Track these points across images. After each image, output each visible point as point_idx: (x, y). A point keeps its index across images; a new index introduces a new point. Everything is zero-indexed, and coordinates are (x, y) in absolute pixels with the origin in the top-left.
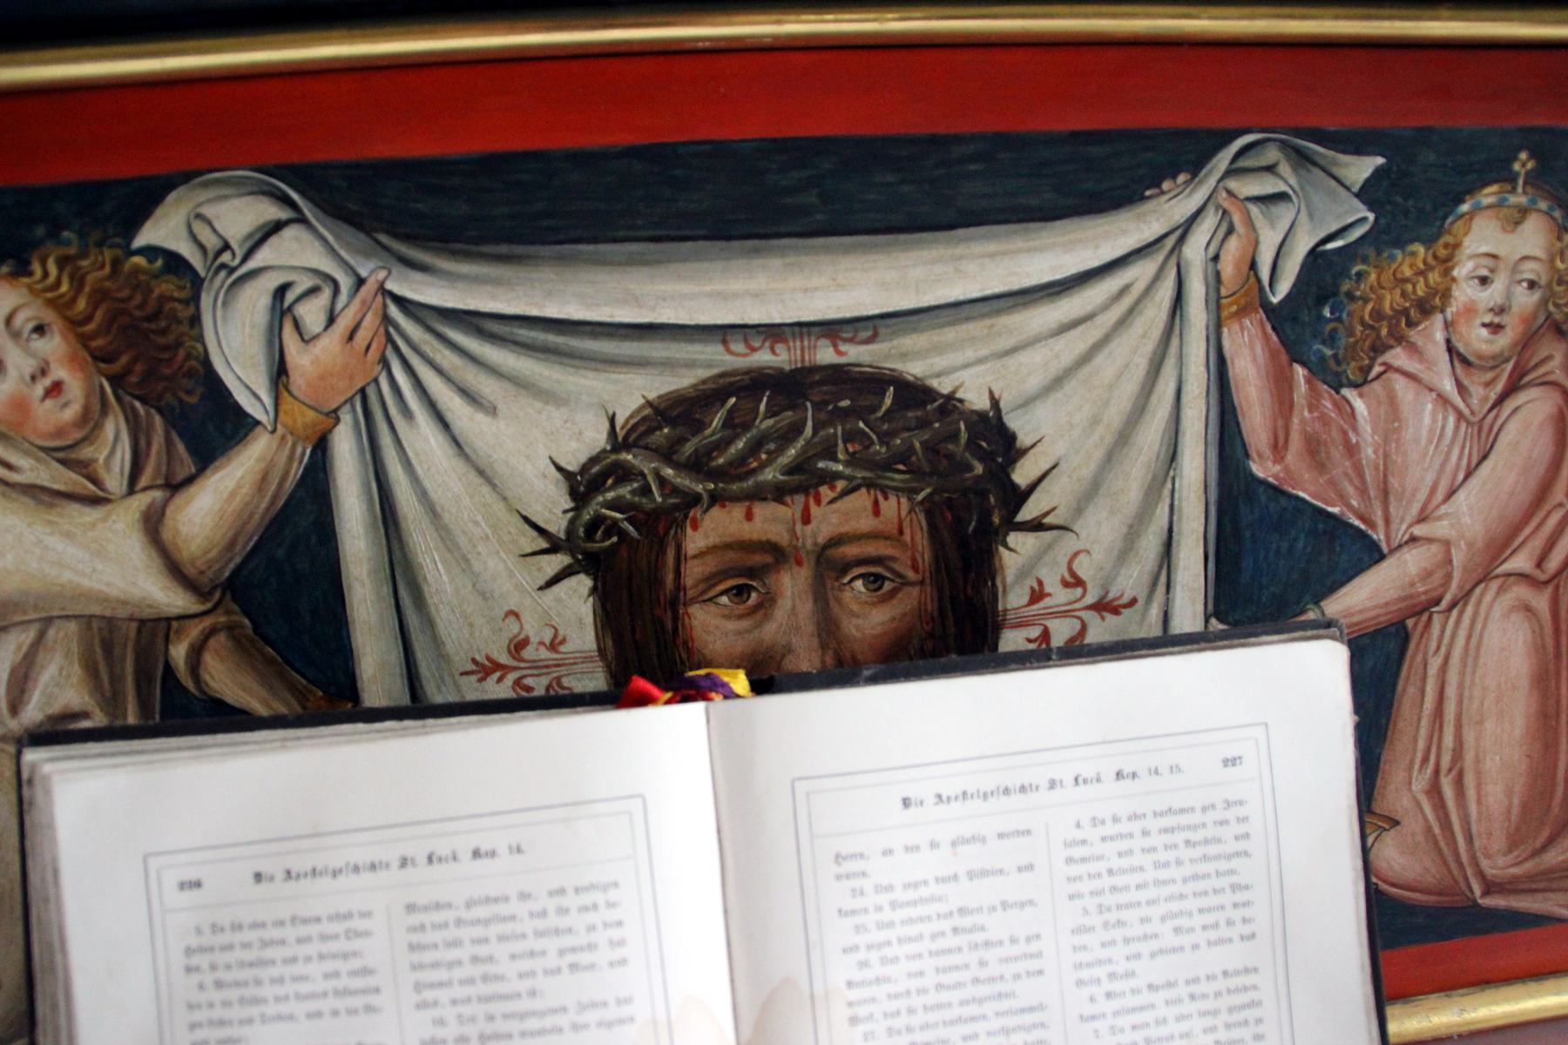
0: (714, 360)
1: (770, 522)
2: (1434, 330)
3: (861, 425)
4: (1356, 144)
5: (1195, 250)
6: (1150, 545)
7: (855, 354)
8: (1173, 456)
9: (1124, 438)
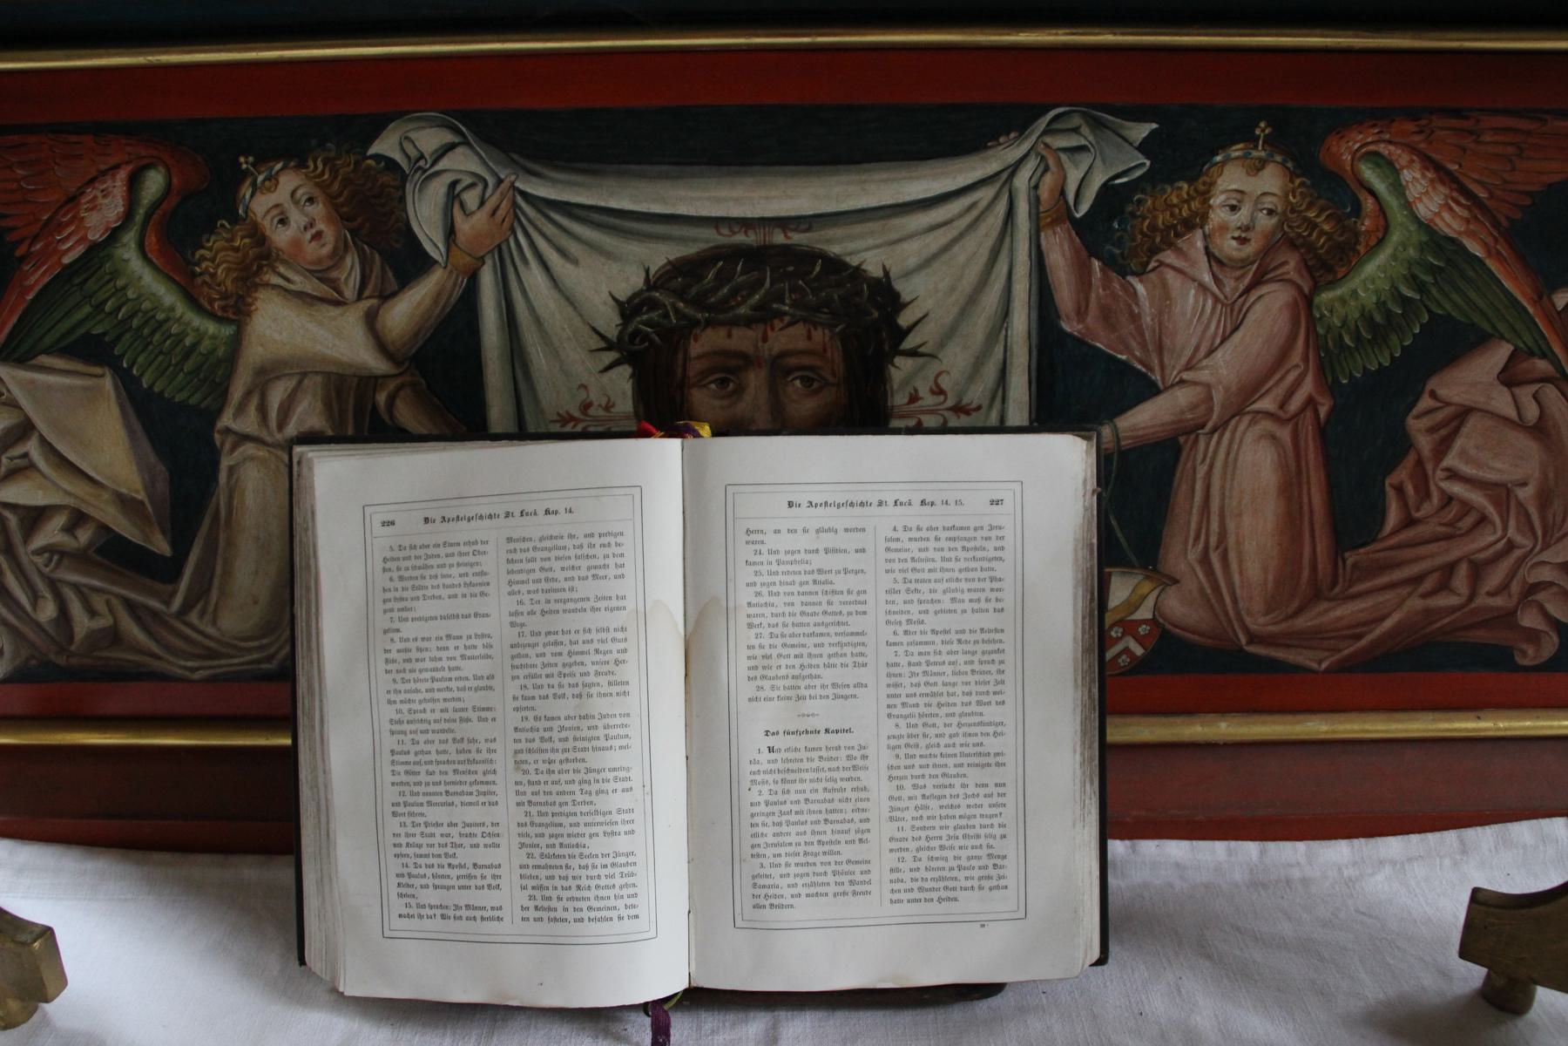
0: (709, 238)
1: (742, 339)
3: (800, 282)
4: (1138, 115)
5: (1022, 181)
6: (990, 371)
7: (797, 238)
8: (1005, 313)
9: (973, 299)
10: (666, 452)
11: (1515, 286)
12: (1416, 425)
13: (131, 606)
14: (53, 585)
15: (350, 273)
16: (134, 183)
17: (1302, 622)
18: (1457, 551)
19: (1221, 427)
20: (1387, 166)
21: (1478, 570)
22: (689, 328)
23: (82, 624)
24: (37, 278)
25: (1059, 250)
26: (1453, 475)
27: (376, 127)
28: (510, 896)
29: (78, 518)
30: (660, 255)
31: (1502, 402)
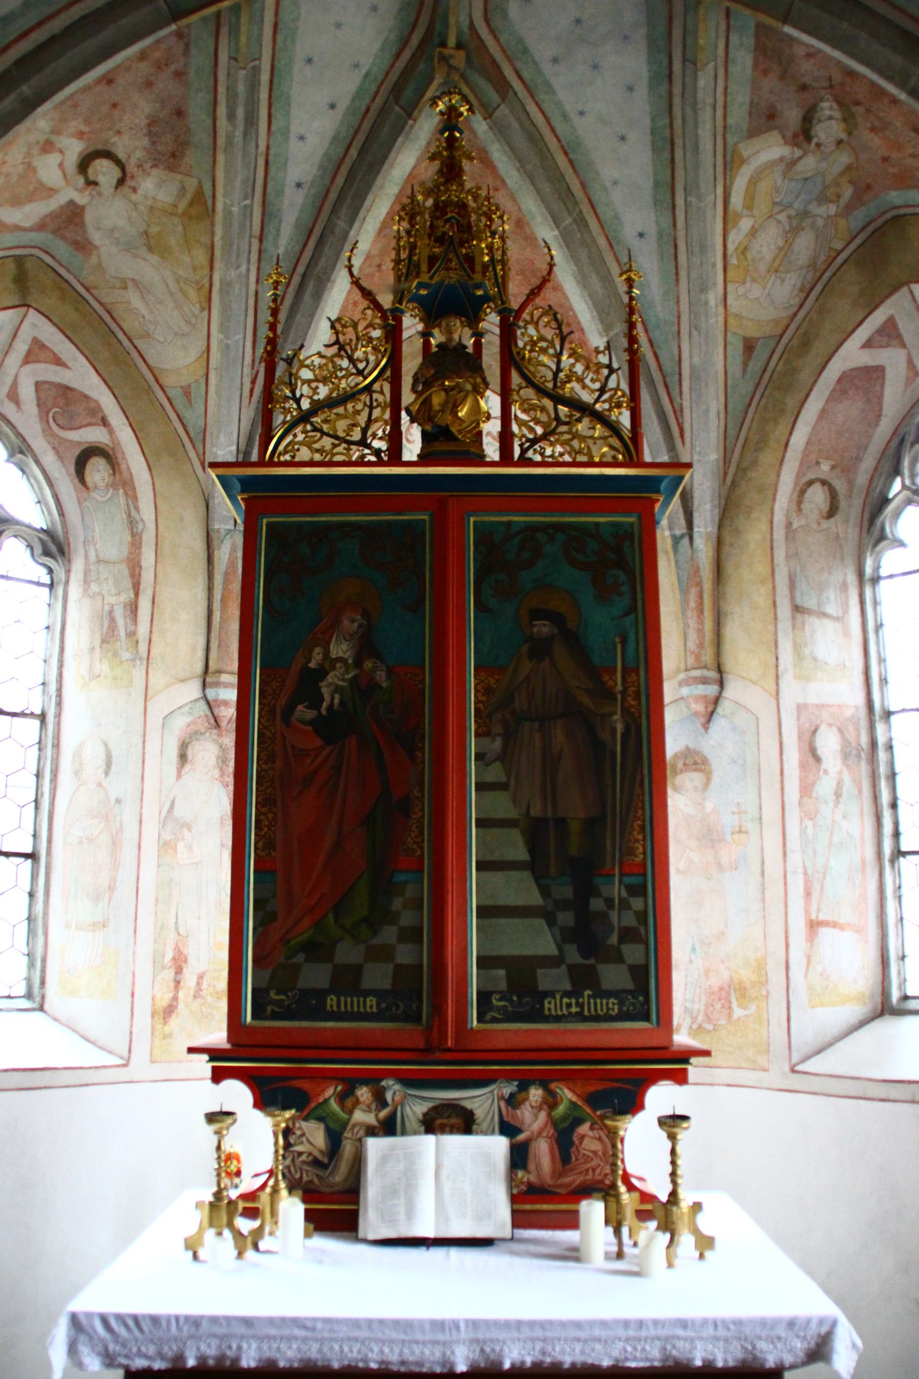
1: (445, 1121)
2: (527, 1103)
4: (515, 1080)
5: (495, 1092)
6: (491, 1127)
7: (455, 1102)
10: (431, 1138)
11: (588, 1110)
12: (575, 1139)
13: (317, 1176)
14: (301, 1170)
15: (374, 1106)
16: (336, 1088)
17: (559, 1182)
18: (588, 1165)
19: (536, 1139)
20: (561, 1089)
21: (594, 1170)
22: (435, 1119)
23: (305, 1178)
24: (313, 1105)
25: (503, 1104)
26: (584, 1149)
27: (382, 1080)
28: (402, 1216)
29: (310, 1154)
30: (430, 1105)
31: (591, 1133)
